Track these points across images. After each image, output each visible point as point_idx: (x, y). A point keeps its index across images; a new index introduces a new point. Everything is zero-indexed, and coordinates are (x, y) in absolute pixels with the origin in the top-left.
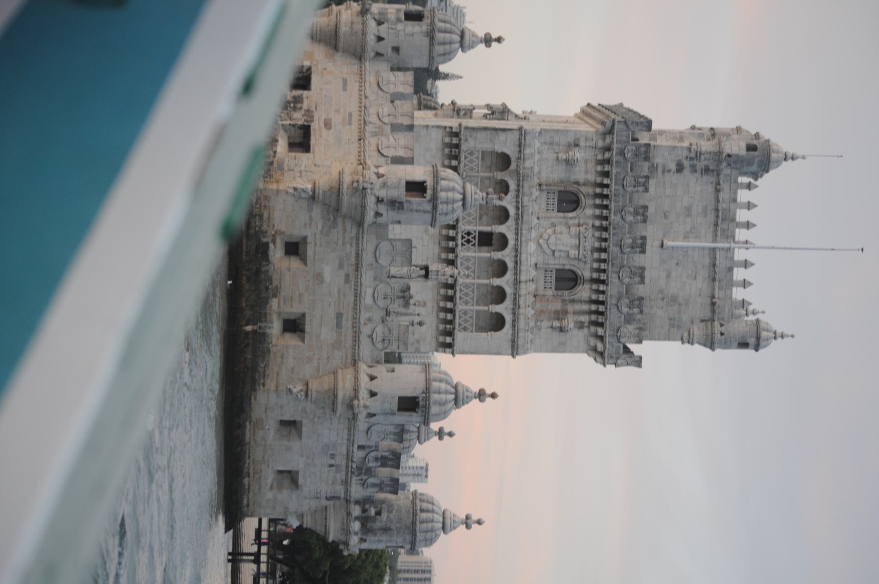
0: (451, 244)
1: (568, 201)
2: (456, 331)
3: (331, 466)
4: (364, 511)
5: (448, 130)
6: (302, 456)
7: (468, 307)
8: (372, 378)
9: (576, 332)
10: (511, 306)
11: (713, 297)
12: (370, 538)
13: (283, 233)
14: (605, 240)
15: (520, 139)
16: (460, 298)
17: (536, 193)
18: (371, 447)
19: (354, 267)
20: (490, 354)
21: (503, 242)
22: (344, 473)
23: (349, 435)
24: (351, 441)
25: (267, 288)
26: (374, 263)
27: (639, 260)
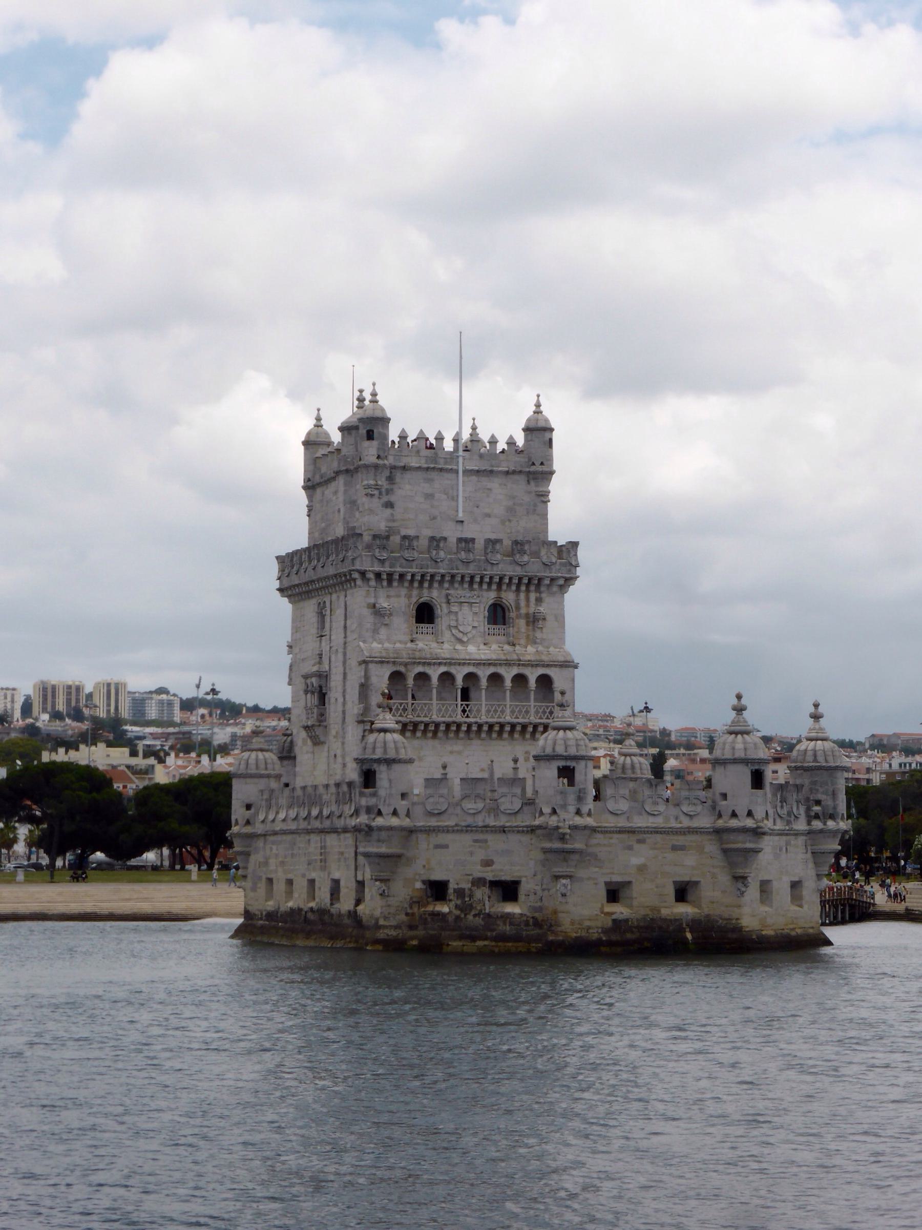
0: (474, 728)
1: (425, 614)
4: (817, 817)
7: (533, 710)
10: (530, 668)
11: (507, 473)
13: (603, 905)
14: (463, 577)
15: (377, 662)
16: (523, 718)
20: (574, 689)
25: (652, 919)
27: (479, 545)
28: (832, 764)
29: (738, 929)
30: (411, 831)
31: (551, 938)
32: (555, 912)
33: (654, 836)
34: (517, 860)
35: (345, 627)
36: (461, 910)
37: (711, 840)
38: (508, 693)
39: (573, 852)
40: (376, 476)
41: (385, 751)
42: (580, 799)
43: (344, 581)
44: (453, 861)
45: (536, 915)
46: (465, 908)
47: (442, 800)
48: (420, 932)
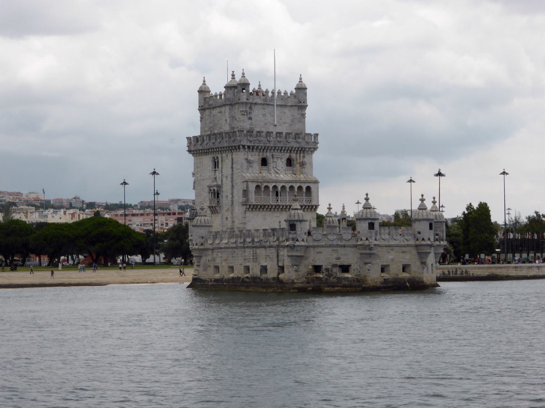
1: (264, 162)
11: (291, 106)
29: (423, 282)
30: (307, 247)
31: (364, 286)
32: (365, 276)
34: (349, 257)
35: (232, 168)
36: (328, 276)
39: (373, 254)
41: (299, 217)
42: (376, 234)
43: (237, 148)
44: (325, 258)
46: (330, 275)
48: (312, 285)
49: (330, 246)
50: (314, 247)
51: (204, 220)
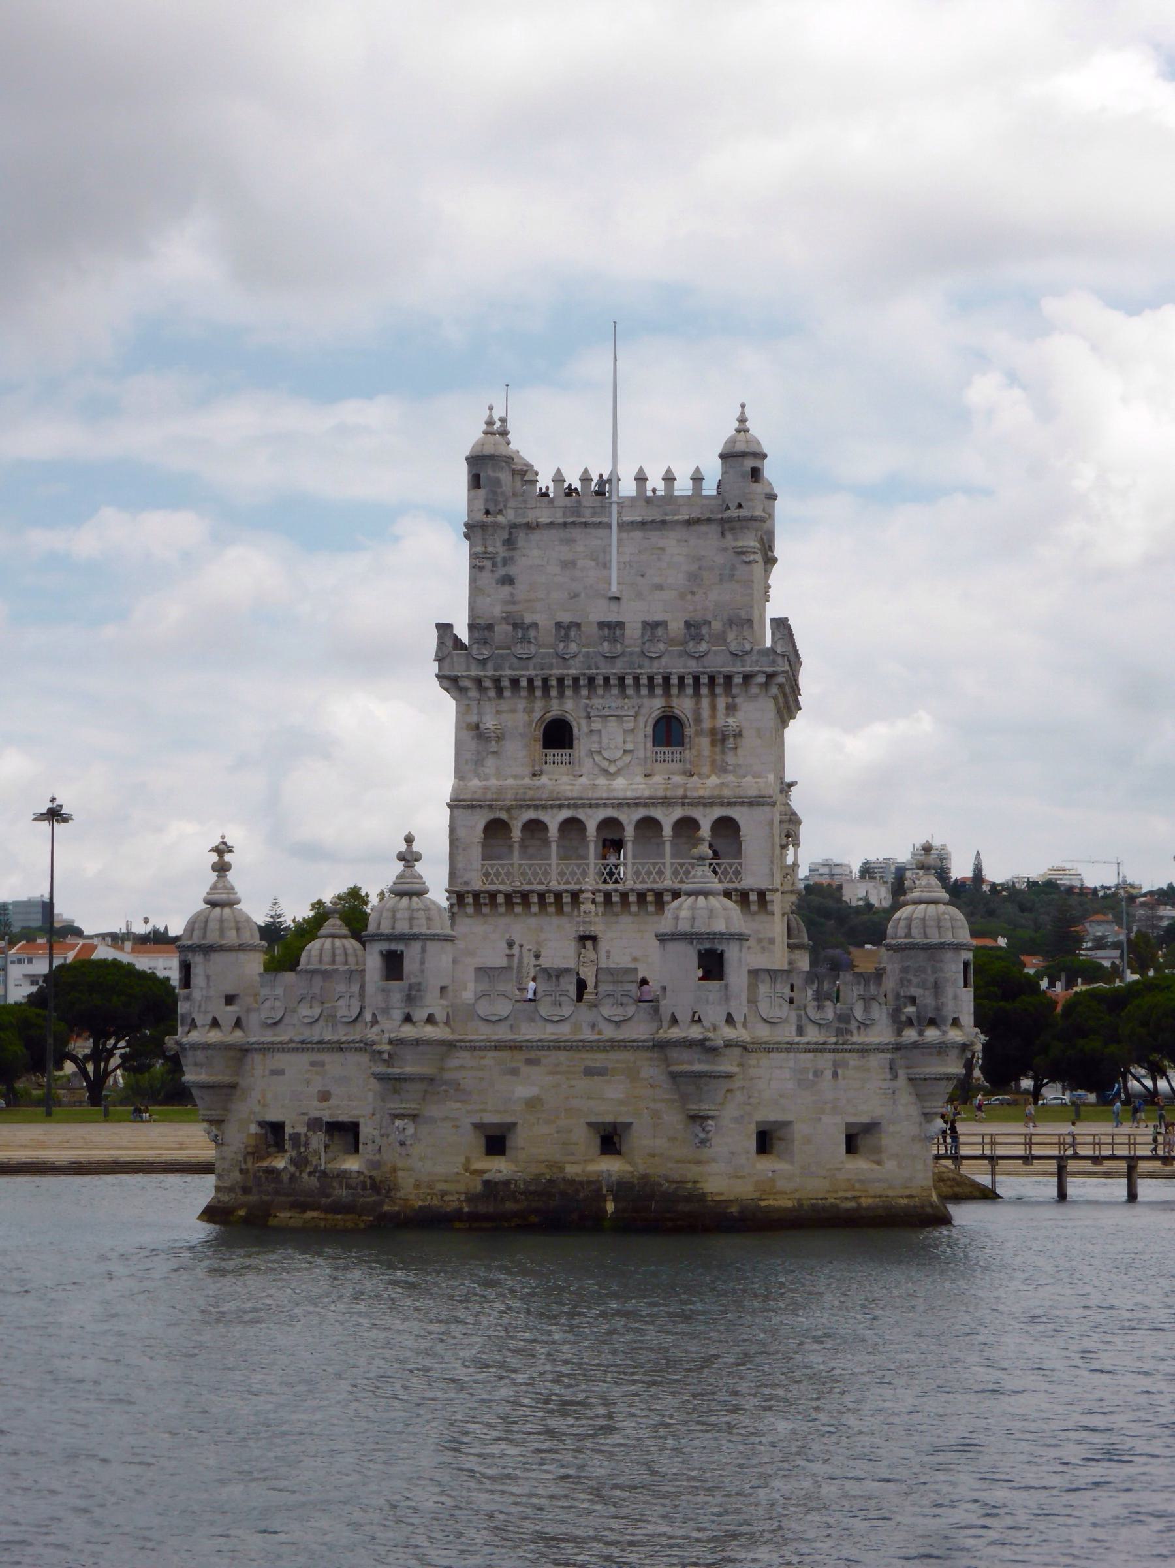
0: (616, 898)
1: (557, 735)
2: (738, 886)
3: (835, 1075)
4: (910, 1023)
5: (455, 910)
6: (820, 1119)
8: (674, 1021)
9: (740, 715)
10: (701, 808)
11: (689, 523)
12: (949, 1012)
13: (468, 1159)
14: (607, 680)
15: (464, 807)
17: (544, 779)
18: (799, 1017)
19: (515, 1052)
21: (610, 824)
22: (847, 1055)
23: (779, 1050)
24: (790, 1047)
25: (550, 1181)
26: (509, 1022)
27: (633, 631)
28: (934, 939)
30: (243, 1051)
31: (386, 1208)
33: (553, 1053)
37: (651, 1059)
38: (668, 846)
40: (484, 539)
45: (374, 1173)
47: (278, 1004)
48: (253, 1198)
49: (303, 1046)
50: (266, 1049)
51: (333, 948)
